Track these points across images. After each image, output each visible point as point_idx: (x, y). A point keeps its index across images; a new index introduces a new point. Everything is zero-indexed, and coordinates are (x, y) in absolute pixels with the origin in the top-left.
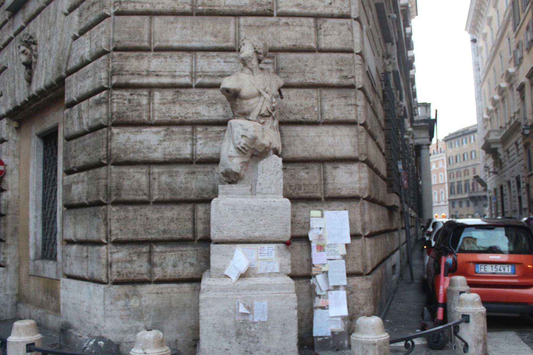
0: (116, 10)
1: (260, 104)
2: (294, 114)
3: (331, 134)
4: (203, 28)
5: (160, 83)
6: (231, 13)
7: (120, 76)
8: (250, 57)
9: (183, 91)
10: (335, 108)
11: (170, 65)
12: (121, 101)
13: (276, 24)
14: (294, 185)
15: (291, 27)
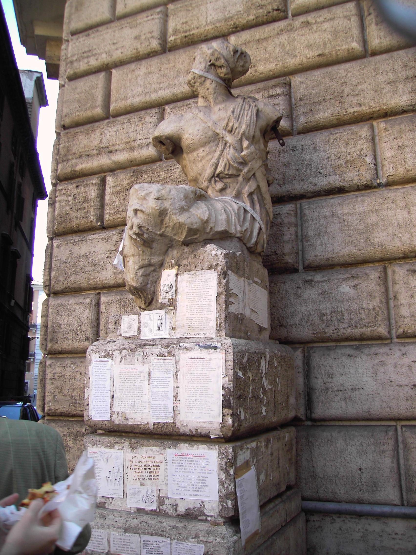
0: (67, 73)
1: (217, 154)
2: (326, 176)
3: (402, 204)
4: (174, 66)
5: (115, 163)
6: (216, 34)
7: (65, 163)
8: (201, 77)
9: (144, 168)
10: (407, 149)
11: (127, 133)
12: (65, 198)
13: (291, 29)
14: (328, 312)
15: (315, 27)
